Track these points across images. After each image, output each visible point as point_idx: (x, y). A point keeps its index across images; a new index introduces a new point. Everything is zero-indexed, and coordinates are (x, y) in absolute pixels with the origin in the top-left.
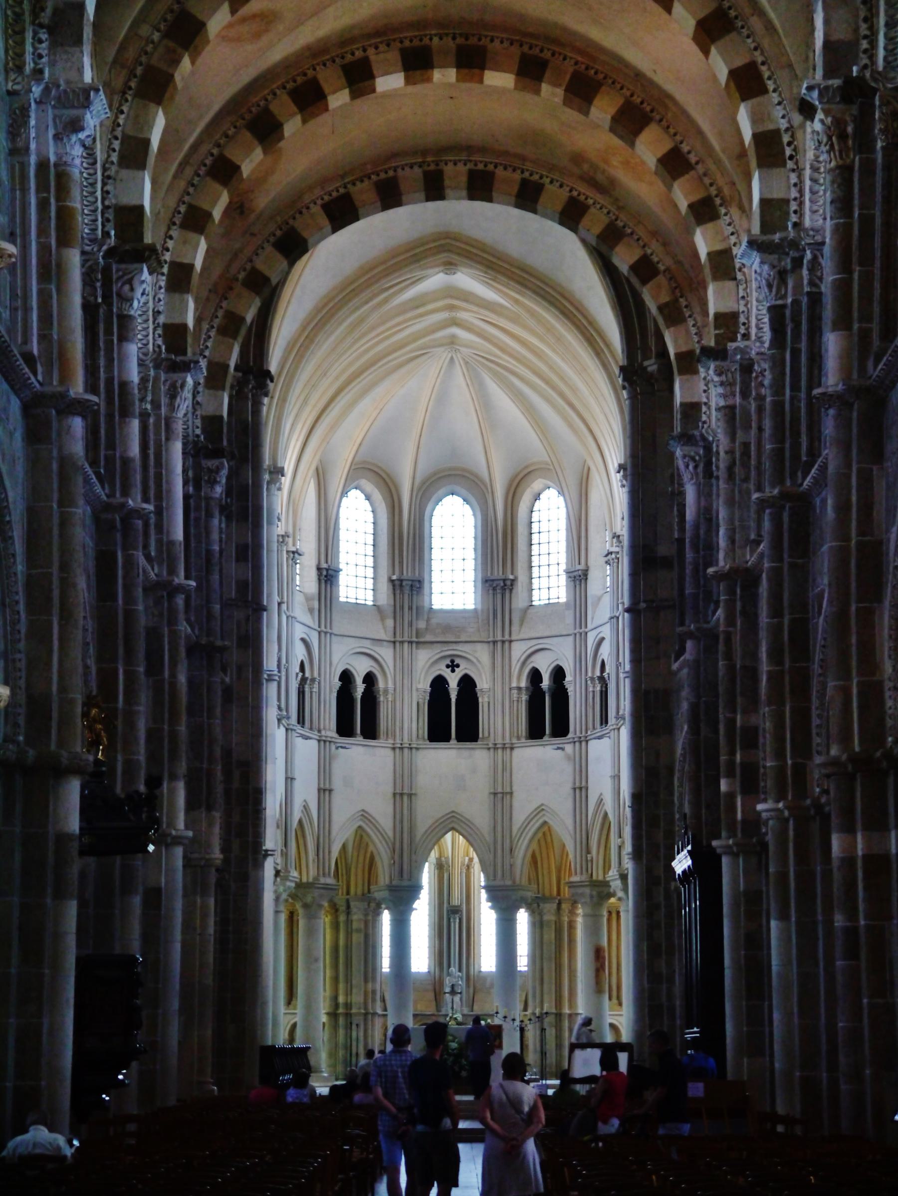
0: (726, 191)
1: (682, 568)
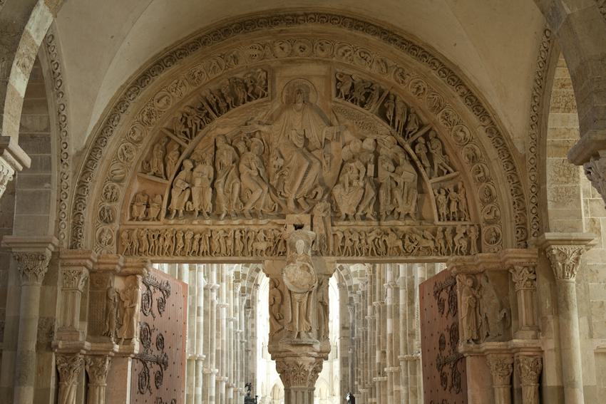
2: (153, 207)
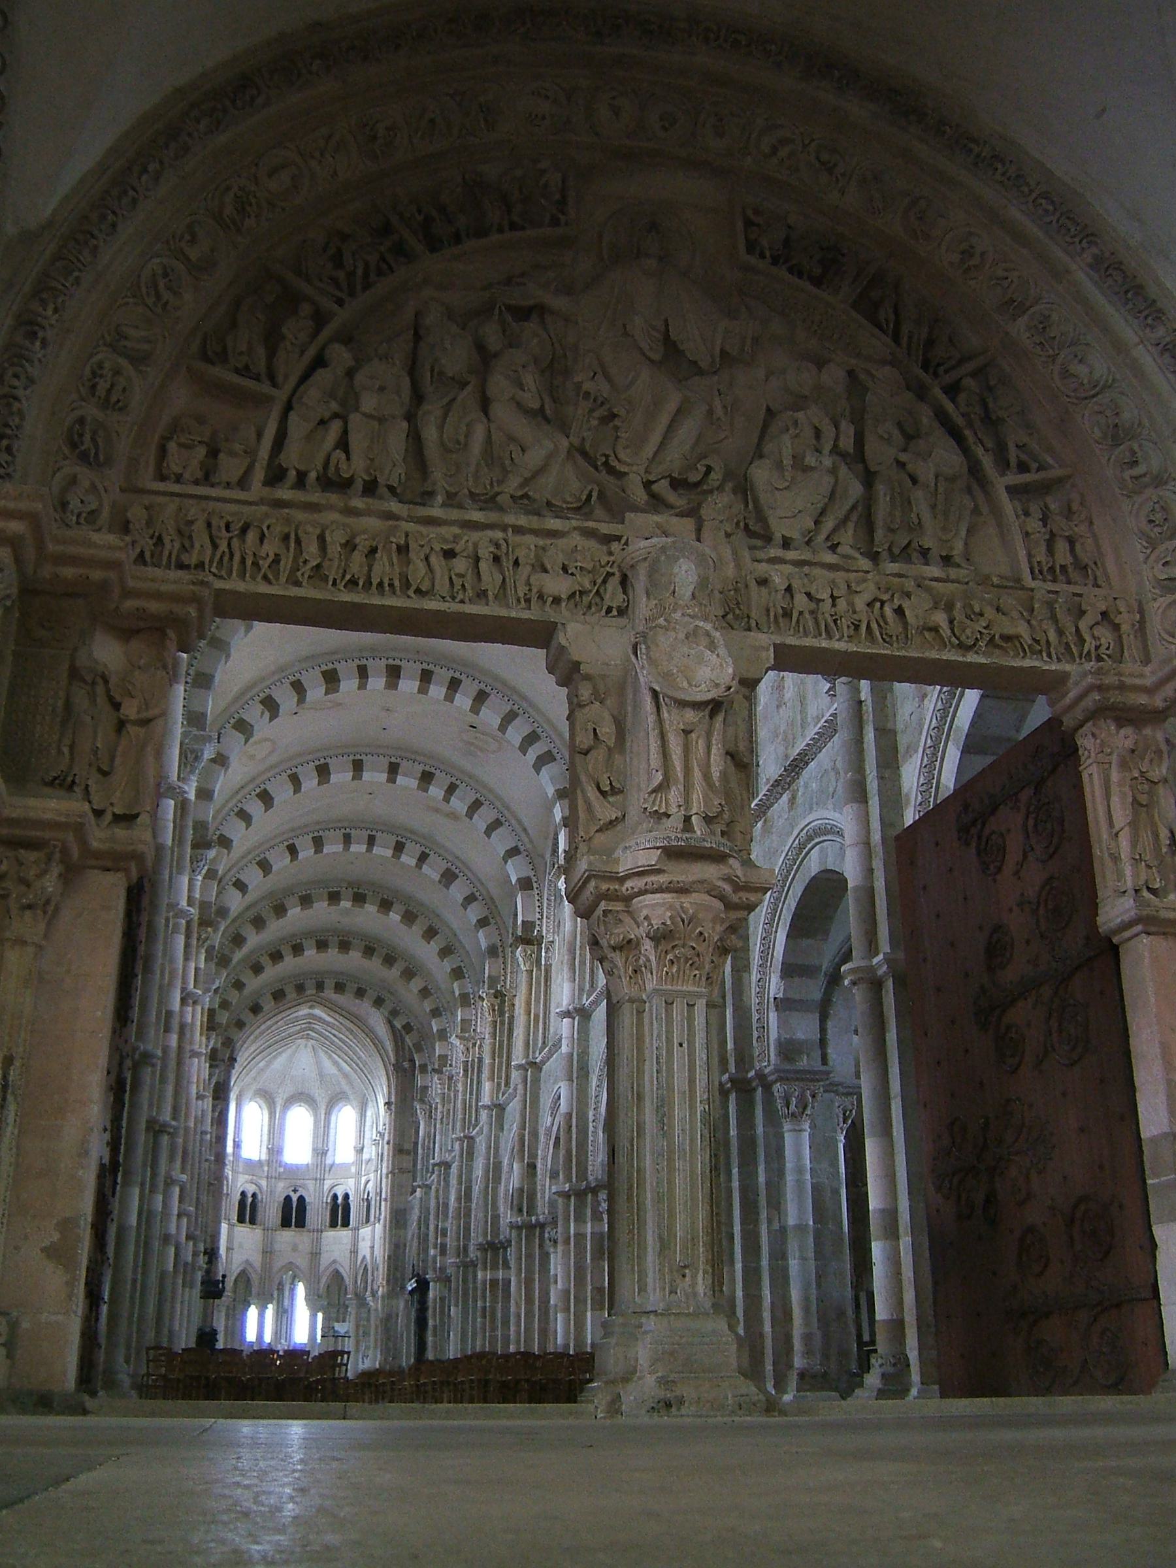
0: (446, 1005)
1: (416, 1153)
2: (232, 454)
